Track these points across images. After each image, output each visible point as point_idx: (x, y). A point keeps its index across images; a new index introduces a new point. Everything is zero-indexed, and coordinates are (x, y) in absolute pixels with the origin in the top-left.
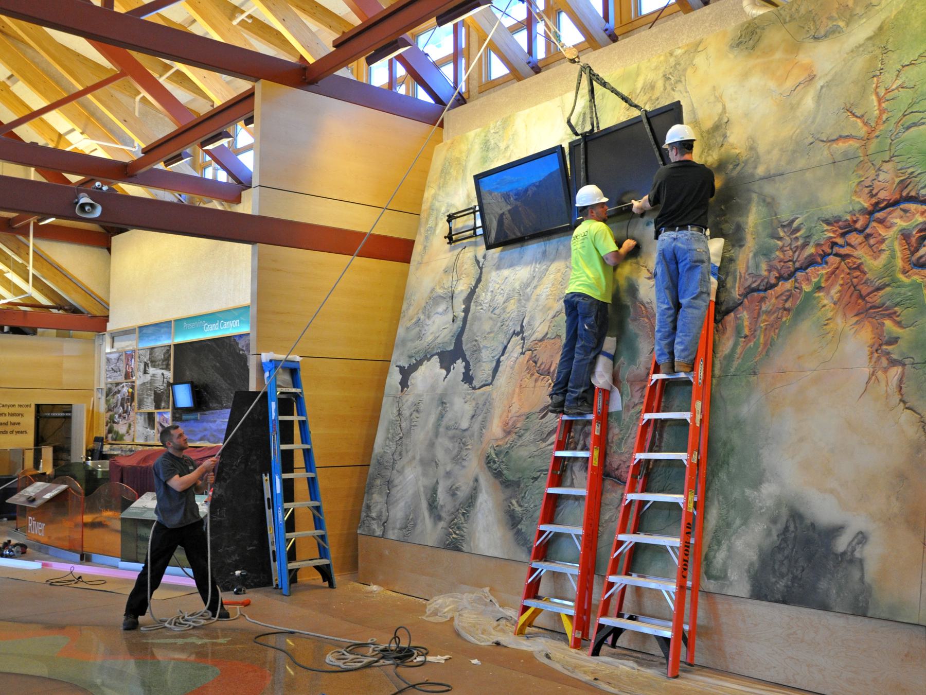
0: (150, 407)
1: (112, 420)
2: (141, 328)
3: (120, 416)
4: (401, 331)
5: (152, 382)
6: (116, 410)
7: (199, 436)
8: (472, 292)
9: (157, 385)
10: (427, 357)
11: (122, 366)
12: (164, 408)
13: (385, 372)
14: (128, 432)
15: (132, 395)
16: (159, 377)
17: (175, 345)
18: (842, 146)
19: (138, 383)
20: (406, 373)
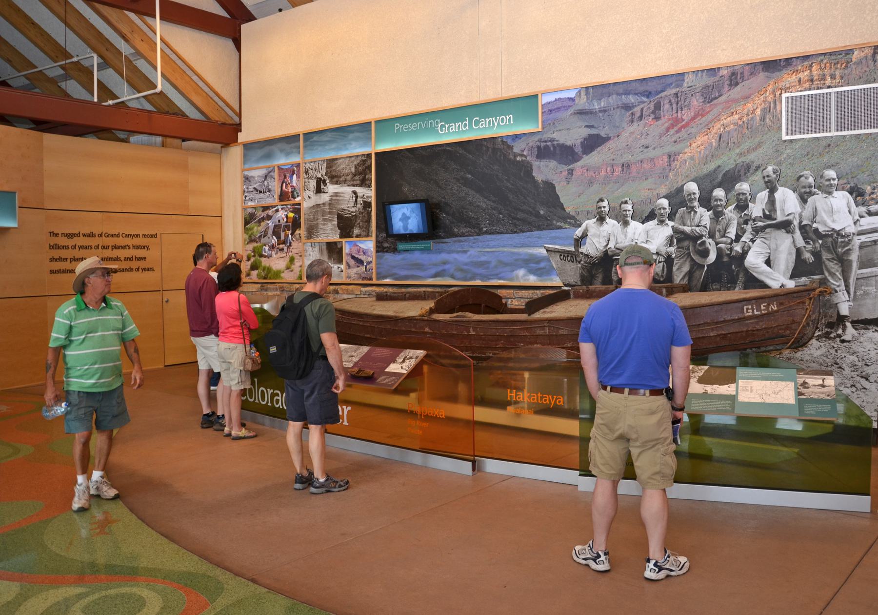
0: (330, 233)
6: (263, 240)
7: (433, 271)
9: (344, 206)
11: (275, 185)
12: (357, 236)
14: (288, 268)
17: (377, 154)
19: (306, 205)
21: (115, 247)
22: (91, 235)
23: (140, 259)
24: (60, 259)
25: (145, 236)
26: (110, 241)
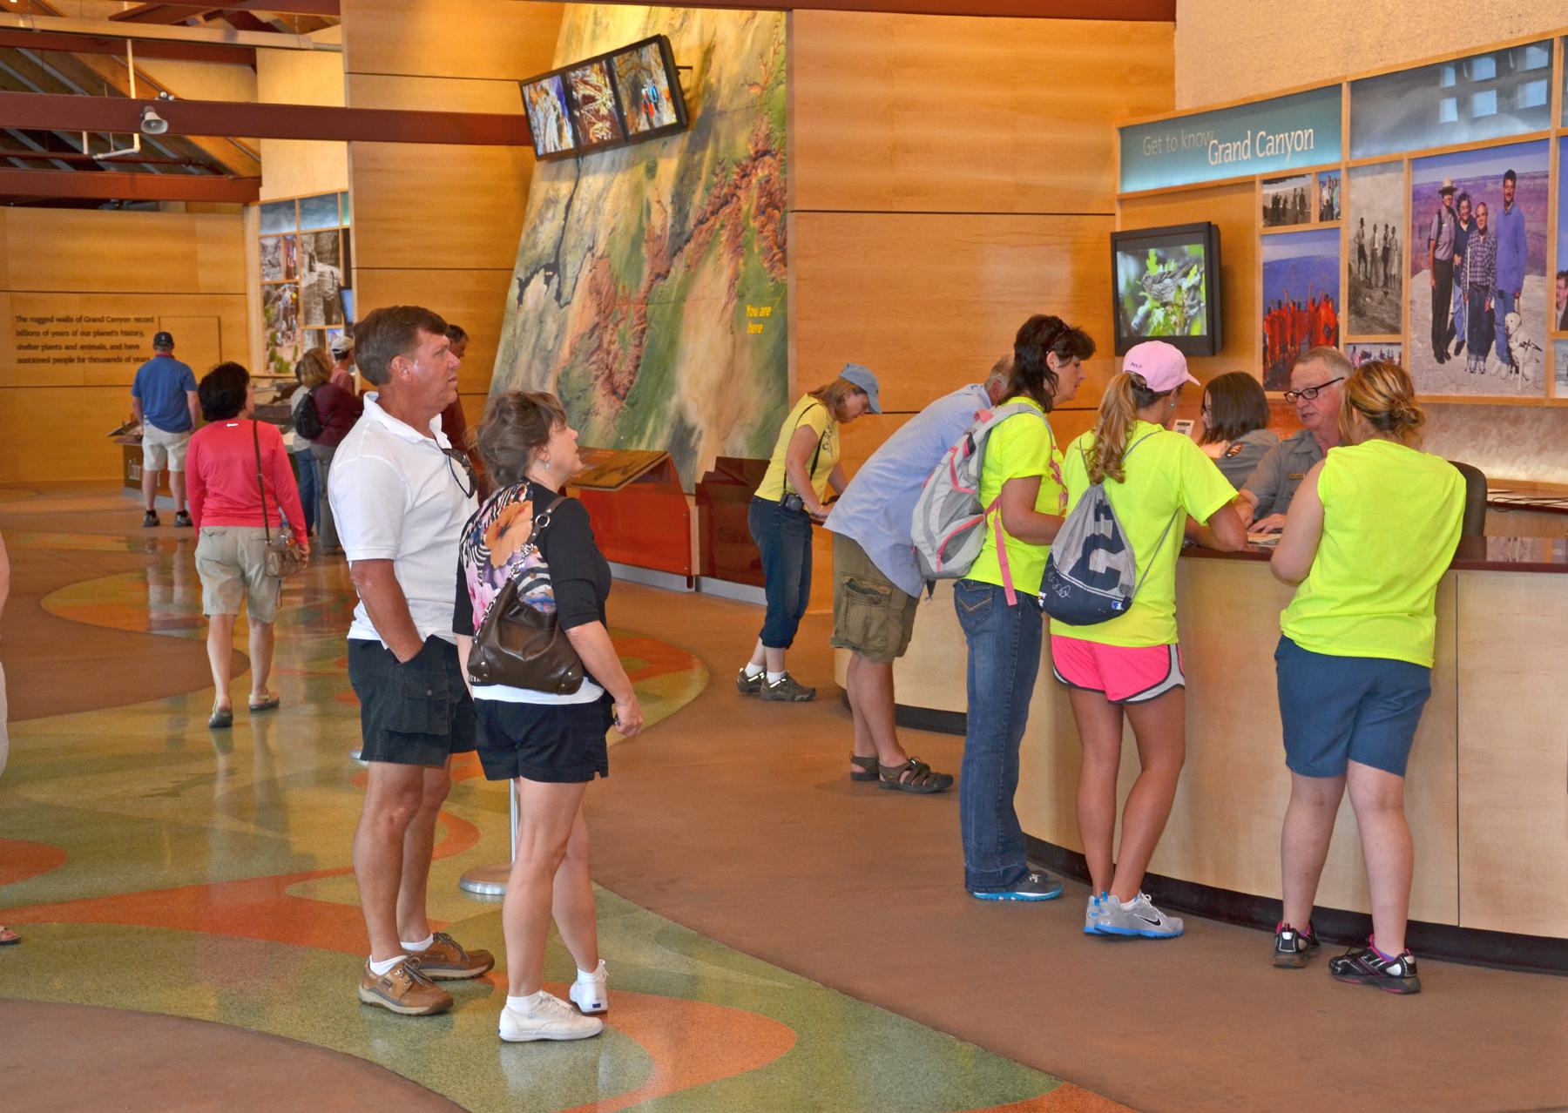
1: (273, 343)
2: (303, 200)
3: (283, 334)
4: (523, 236)
5: (320, 284)
8: (571, 199)
10: (537, 271)
11: (281, 256)
13: (508, 285)
15: (296, 302)
16: (328, 277)
18: (755, 91)
19: (303, 284)
20: (524, 285)
22: (68, 320)
23: (130, 347)
24: (29, 347)
25: (138, 320)
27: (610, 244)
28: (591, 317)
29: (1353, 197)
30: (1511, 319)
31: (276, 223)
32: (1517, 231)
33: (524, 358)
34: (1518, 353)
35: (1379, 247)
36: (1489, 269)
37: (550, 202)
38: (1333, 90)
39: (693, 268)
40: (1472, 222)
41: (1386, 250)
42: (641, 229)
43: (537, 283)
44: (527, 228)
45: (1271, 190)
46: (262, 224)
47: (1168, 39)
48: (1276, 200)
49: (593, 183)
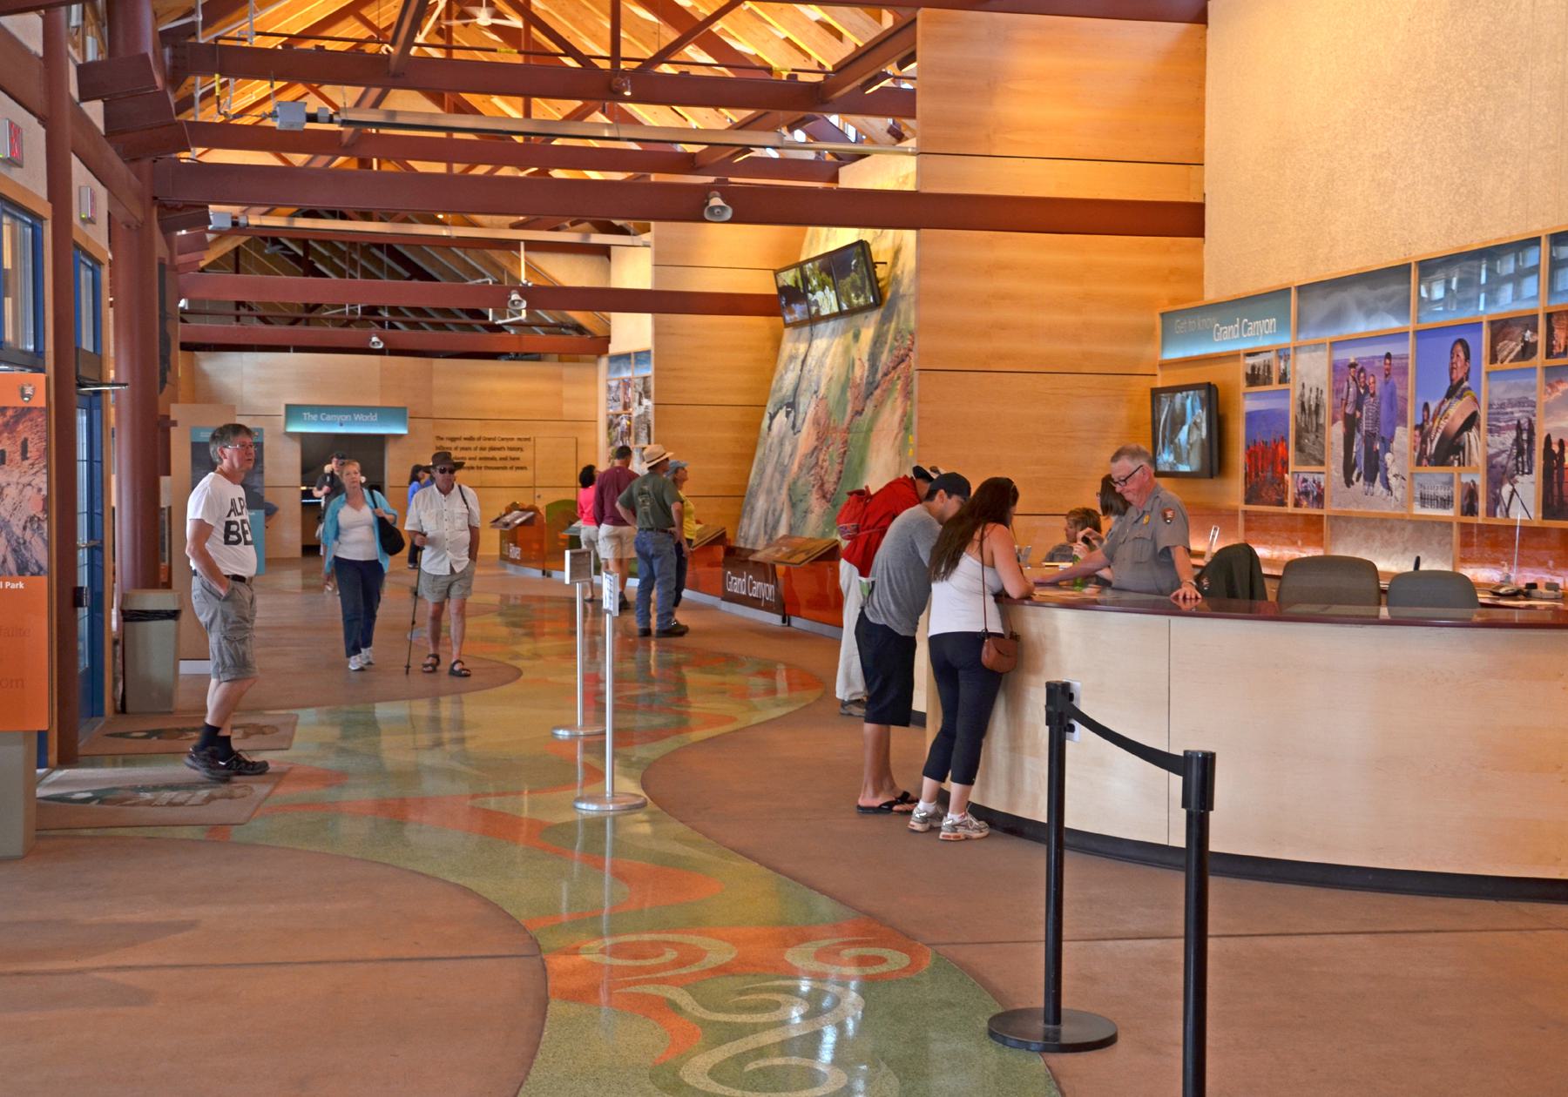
2: (637, 353)
11: (621, 394)
15: (629, 427)
19: (635, 415)
20: (772, 417)
21: (492, 449)
22: (471, 439)
26: (487, 444)
27: (828, 389)
28: (813, 442)
29: (1298, 367)
30: (1388, 456)
31: (618, 370)
32: (1392, 394)
33: (769, 470)
34: (1393, 481)
35: (1313, 403)
36: (1376, 422)
37: (792, 358)
38: (1286, 291)
39: (878, 407)
40: (1366, 388)
41: (1317, 406)
42: (848, 379)
43: (781, 416)
44: (776, 377)
45: (1251, 361)
46: (609, 369)
47: (1199, 250)
48: (1253, 368)
49: (820, 344)
